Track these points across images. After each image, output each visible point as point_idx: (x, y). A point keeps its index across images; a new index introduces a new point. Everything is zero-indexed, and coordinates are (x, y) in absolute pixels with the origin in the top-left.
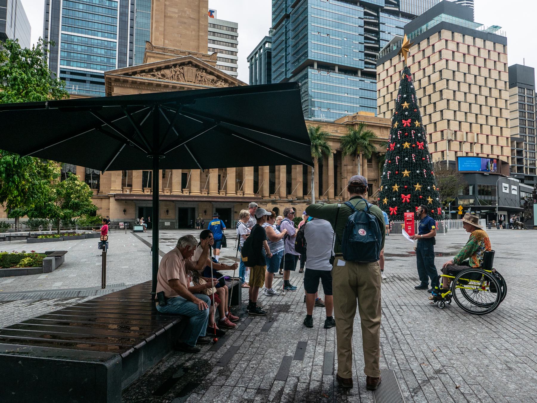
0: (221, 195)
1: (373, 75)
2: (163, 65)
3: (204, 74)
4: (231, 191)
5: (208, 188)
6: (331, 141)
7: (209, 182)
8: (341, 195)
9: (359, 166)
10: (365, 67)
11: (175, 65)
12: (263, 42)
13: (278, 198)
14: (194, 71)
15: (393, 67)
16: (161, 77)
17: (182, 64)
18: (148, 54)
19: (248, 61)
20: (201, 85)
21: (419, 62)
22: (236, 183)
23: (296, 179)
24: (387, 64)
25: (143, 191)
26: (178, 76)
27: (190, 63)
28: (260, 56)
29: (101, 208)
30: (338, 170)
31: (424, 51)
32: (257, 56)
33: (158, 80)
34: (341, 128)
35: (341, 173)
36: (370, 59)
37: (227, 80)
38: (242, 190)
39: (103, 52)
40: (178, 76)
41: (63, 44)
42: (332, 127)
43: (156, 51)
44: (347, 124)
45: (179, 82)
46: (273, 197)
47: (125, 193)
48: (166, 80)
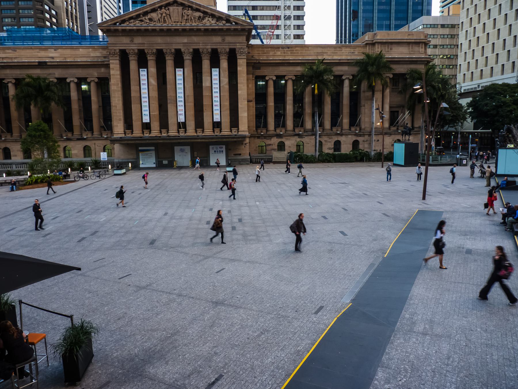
3: (190, 12)
6: (345, 65)
8: (359, 125)
11: (160, 7)
16: (148, 21)
17: (168, 5)
26: (164, 18)
34: (360, 49)
40: (164, 18)
44: (367, 44)
46: (278, 131)
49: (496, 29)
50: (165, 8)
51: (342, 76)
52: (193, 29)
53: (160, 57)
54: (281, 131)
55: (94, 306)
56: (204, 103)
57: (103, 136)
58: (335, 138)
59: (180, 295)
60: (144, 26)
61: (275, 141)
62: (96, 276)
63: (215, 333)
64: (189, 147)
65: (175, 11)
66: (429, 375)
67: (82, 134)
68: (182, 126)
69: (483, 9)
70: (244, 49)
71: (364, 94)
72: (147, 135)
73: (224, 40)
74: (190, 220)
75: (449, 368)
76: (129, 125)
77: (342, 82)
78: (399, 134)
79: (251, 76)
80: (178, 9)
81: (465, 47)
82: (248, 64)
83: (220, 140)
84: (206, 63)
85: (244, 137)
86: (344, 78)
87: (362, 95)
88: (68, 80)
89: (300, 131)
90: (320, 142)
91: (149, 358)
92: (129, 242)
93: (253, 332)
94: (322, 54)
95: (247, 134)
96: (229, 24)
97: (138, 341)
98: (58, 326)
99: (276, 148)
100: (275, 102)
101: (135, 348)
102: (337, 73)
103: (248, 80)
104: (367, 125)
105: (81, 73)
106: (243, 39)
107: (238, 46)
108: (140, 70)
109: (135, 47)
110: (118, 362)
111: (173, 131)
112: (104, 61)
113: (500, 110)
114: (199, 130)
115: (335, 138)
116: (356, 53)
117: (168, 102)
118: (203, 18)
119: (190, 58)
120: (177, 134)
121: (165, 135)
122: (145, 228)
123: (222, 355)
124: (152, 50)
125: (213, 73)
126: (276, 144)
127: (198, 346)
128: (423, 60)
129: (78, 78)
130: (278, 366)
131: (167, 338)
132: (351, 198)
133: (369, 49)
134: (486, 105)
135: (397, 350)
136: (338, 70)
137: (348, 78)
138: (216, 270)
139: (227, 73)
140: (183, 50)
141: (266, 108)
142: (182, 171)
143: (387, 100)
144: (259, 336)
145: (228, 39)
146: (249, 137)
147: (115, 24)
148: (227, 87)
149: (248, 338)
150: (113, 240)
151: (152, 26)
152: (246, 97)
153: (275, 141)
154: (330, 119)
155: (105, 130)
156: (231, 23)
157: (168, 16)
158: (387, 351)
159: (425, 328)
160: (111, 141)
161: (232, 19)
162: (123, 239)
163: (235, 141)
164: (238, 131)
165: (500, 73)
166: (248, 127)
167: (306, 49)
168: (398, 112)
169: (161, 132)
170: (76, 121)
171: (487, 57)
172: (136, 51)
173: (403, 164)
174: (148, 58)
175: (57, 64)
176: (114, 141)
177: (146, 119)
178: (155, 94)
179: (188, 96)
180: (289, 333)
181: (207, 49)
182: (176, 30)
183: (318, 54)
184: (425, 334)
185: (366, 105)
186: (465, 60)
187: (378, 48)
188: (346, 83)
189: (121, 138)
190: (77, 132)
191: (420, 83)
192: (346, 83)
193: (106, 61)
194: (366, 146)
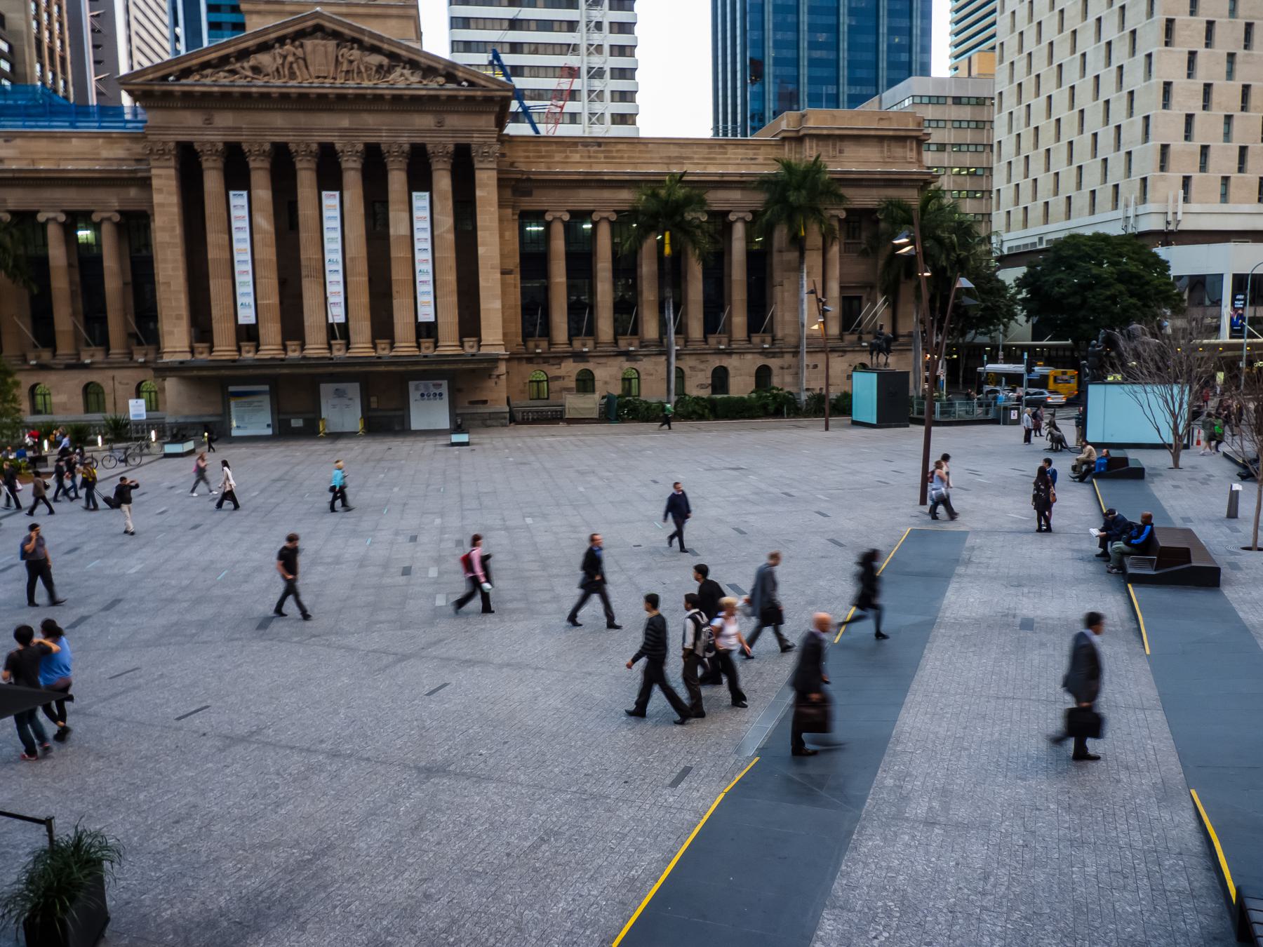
3: (356, 53)
8: (770, 330)
11: (281, 41)
16: (249, 73)
25: (239, 350)
26: (291, 67)
27: (318, 30)
34: (769, 149)
40: (291, 67)
44: (784, 139)
46: (577, 344)
49: (1076, 110)
50: (293, 41)
51: (728, 213)
52: (363, 96)
53: (282, 163)
54: (584, 345)
55: (111, 792)
56: (394, 277)
57: (135, 357)
58: (716, 362)
59: (334, 755)
60: (239, 84)
61: (570, 369)
62: (117, 713)
63: (425, 846)
64: (357, 386)
66: (941, 919)
67: (78, 355)
68: (339, 333)
69: (1046, 63)
70: (490, 146)
71: (781, 257)
72: (250, 355)
73: (440, 124)
74: (361, 566)
75: (988, 901)
76: (202, 330)
77: (729, 227)
78: (863, 350)
79: (510, 211)
80: (324, 46)
81: (1008, 149)
82: (502, 184)
83: (433, 367)
84: (397, 180)
85: (495, 360)
86: (732, 217)
87: (776, 258)
88: (41, 218)
89: (631, 345)
90: (680, 371)
91: (256, 918)
92: (203, 625)
93: (520, 838)
94: (680, 160)
95: (501, 351)
97: (227, 877)
98: (14, 847)
99: (573, 385)
100: (569, 276)
101: (220, 893)
102: (716, 207)
103: (501, 220)
104: (789, 330)
105: (75, 199)
106: (488, 122)
107: (476, 139)
108: (231, 193)
109: (218, 138)
110: (175, 932)
111: (315, 345)
112: (135, 171)
113: (1089, 294)
114: (383, 344)
115: (716, 362)
116: (761, 159)
117: (304, 273)
118: (390, 70)
119: (358, 165)
120: (326, 353)
121: (296, 354)
122: (246, 587)
123: (445, 900)
124: (261, 145)
125: (416, 204)
126: (574, 377)
127: (383, 880)
128: (915, 177)
129: (68, 213)
130: (583, 919)
131: (302, 865)
132: (754, 503)
133: (790, 150)
134: (1059, 283)
135: (866, 865)
136: (717, 199)
137: (743, 219)
138: (427, 689)
139: (450, 203)
140: (338, 147)
141: (546, 290)
142: (341, 444)
143: (835, 272)
144: (535, 848)
145: (453, 121)
146: (508, 360)
147: (164, 78)
148: (451, 237)
149: (508, 855)
150: (161, 621)
151: (259, 85)
152: (497, 261)
153: (570, 369)
154: (701, 316)
155: (140, 343)
156: (459, 84)
157: (301, 62)
158: (843, 868)
159: (931, 808)
160: (155, 370)
161: (460, 74)
162: (188, 617)
163: (473, 370)
164: (480, 346)
165: (1087, 210)
166: (505, 335)
167: (642, 148)
168: (860, 298)
169: (285, 349)
170: (64, 319)
171: (1057, 174)
172: (220, 147)
173: (875, 422)
174: (252, 165)
175: (10, 175)
176: (164, 371)
177: (246, 316)
178: (269, 253)
179: (352, 259)
180: (610, 837)
181: (400, 146)
182: (322, 97)
183: (670, 160)
184: (930, 823)
185: (786, 283)
186: (1009, 181)
187: (811, 148)
188: (739, 231)
189: (182, 363)
190: (65, 347)
191: (907, 232)
192: (739, 231)
193: (141, 170)
194: (788, 379)
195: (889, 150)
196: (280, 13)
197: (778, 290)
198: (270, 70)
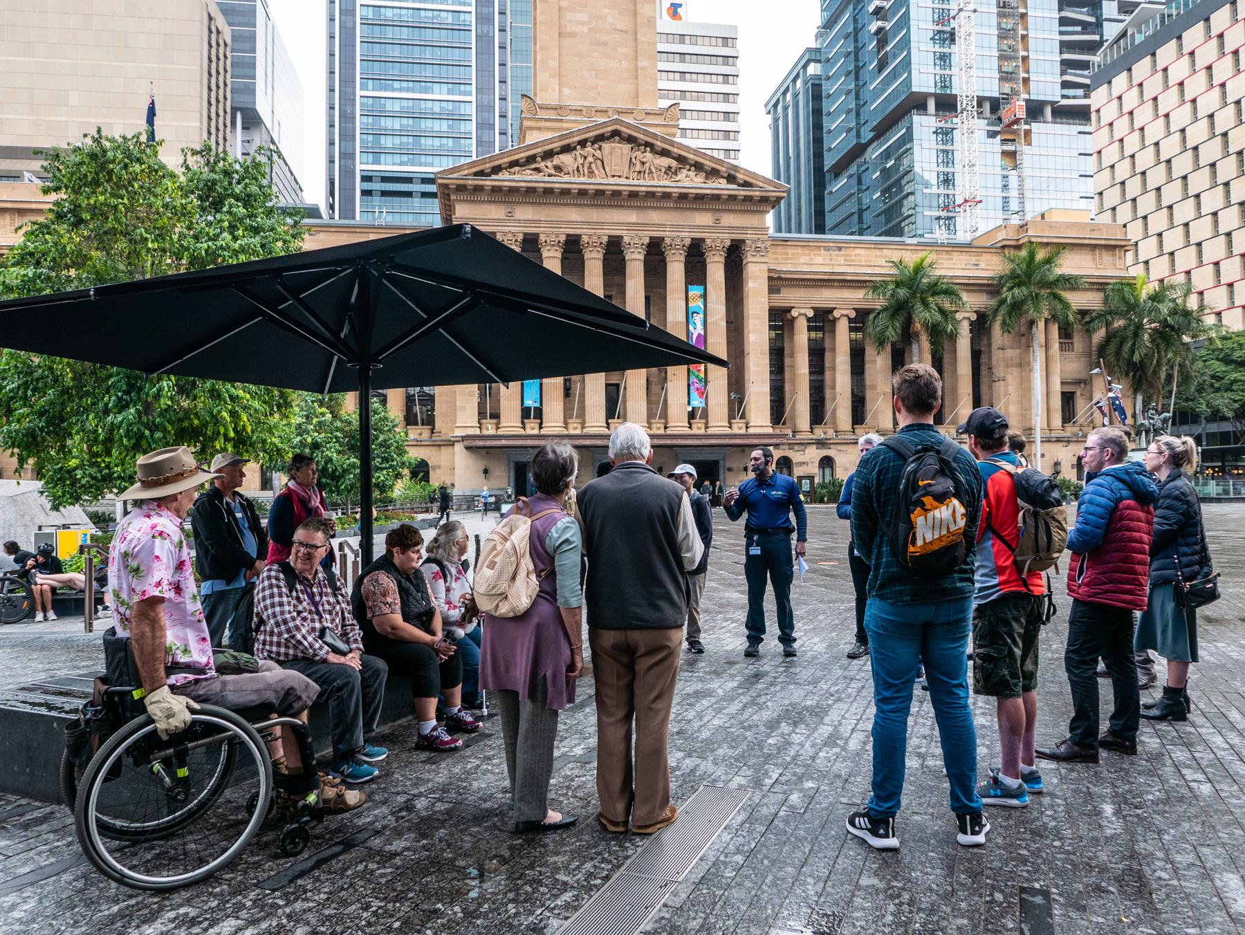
0: (695, 431)
1: (1081, 114)
2: (556, 145)
3: (649, 155)
4: (719, 423)
5: (664, 415)
7: (666, 401)
9: (1036, 347)
10: (1063, 97)
11: (583, 143)
12: (802, 63)
13: (831, 433)
14: (625, 152)
15: (1135, 90)
16: (553, 172)
17: (600, 138)
18: (526, 123)
19: (769, 113)
20: (641, 182)
21: (1209, 68)
22: (730, 402)
23: (874, 387)
24: (1120, 82)
25: (524, 428)
26: (590, 167)
27: (616, 133)
28: (796, 96)
29: (439, 467)
30: (983, 360)
31: (1221, 36)
32: (789, 96)
33: (547, 179)
34: (989, 256)
35: (990, 368)
36: (1075, 75)
37: (701, 164)
38: (743, 417)
39: (444, 126)
40: (590, 167)
41: (365, 119)
42: (965, 257)
43: (542, 114)
44: (1003, 247)
45: (593, 180)
46: (819, 433)
47: (485, 432)
48: (566, 178)
65: (616, 153)
84: (676, 270)
96: (735, 187)
107: (749, 236)
118: (675, 173)
119: (642, 257)
140: (626, 239)
145: (729, 220)
148: (724, 324)
151: (559, 182)
153: (813, 455)
157: (599, 162)
161: (740, 176)
167: (877, 252)
182: (616, 194)
185: (1010, 378)
195: (1101, 258)
196: (559, 129)
197: (999, 387)
198: (570, 170)
